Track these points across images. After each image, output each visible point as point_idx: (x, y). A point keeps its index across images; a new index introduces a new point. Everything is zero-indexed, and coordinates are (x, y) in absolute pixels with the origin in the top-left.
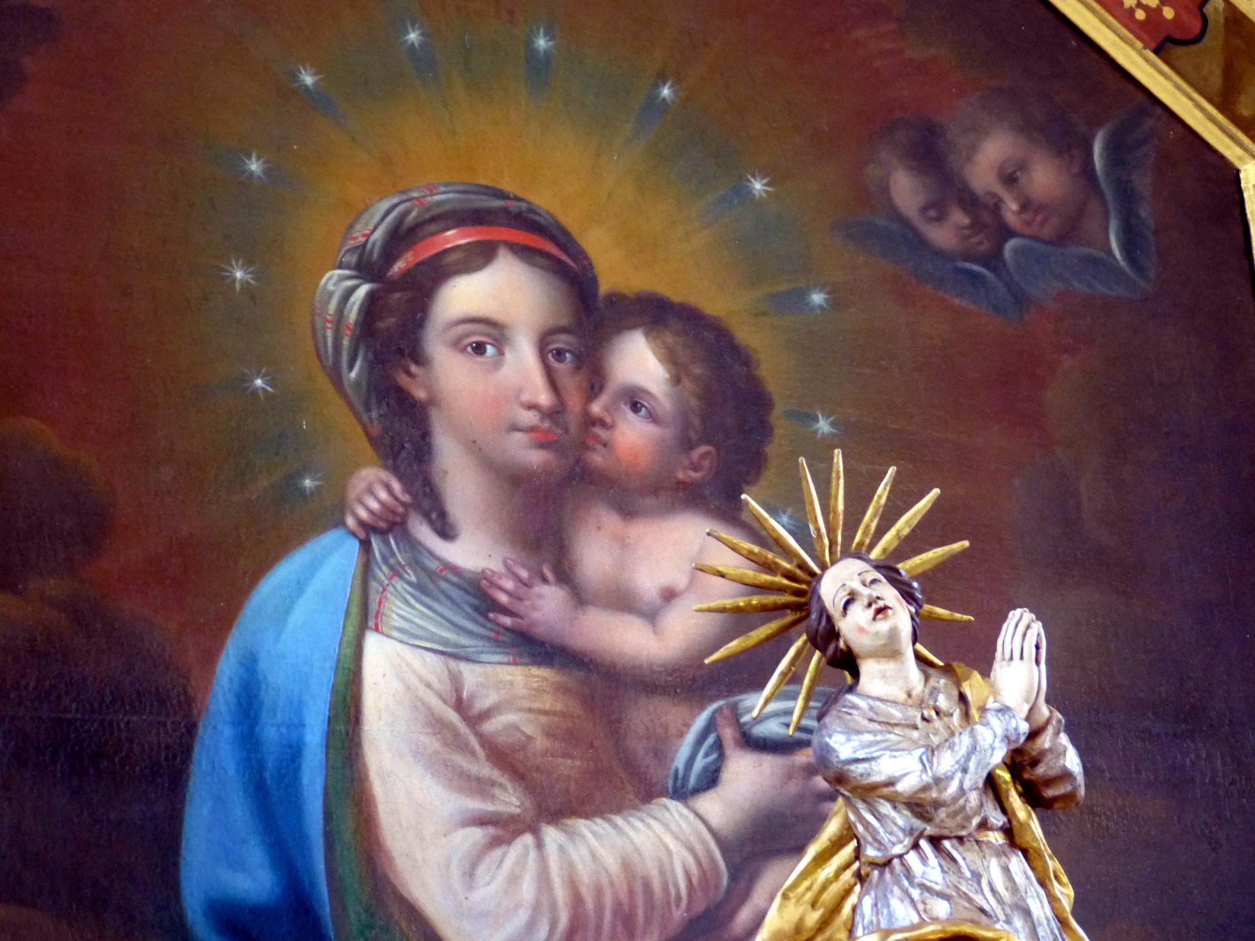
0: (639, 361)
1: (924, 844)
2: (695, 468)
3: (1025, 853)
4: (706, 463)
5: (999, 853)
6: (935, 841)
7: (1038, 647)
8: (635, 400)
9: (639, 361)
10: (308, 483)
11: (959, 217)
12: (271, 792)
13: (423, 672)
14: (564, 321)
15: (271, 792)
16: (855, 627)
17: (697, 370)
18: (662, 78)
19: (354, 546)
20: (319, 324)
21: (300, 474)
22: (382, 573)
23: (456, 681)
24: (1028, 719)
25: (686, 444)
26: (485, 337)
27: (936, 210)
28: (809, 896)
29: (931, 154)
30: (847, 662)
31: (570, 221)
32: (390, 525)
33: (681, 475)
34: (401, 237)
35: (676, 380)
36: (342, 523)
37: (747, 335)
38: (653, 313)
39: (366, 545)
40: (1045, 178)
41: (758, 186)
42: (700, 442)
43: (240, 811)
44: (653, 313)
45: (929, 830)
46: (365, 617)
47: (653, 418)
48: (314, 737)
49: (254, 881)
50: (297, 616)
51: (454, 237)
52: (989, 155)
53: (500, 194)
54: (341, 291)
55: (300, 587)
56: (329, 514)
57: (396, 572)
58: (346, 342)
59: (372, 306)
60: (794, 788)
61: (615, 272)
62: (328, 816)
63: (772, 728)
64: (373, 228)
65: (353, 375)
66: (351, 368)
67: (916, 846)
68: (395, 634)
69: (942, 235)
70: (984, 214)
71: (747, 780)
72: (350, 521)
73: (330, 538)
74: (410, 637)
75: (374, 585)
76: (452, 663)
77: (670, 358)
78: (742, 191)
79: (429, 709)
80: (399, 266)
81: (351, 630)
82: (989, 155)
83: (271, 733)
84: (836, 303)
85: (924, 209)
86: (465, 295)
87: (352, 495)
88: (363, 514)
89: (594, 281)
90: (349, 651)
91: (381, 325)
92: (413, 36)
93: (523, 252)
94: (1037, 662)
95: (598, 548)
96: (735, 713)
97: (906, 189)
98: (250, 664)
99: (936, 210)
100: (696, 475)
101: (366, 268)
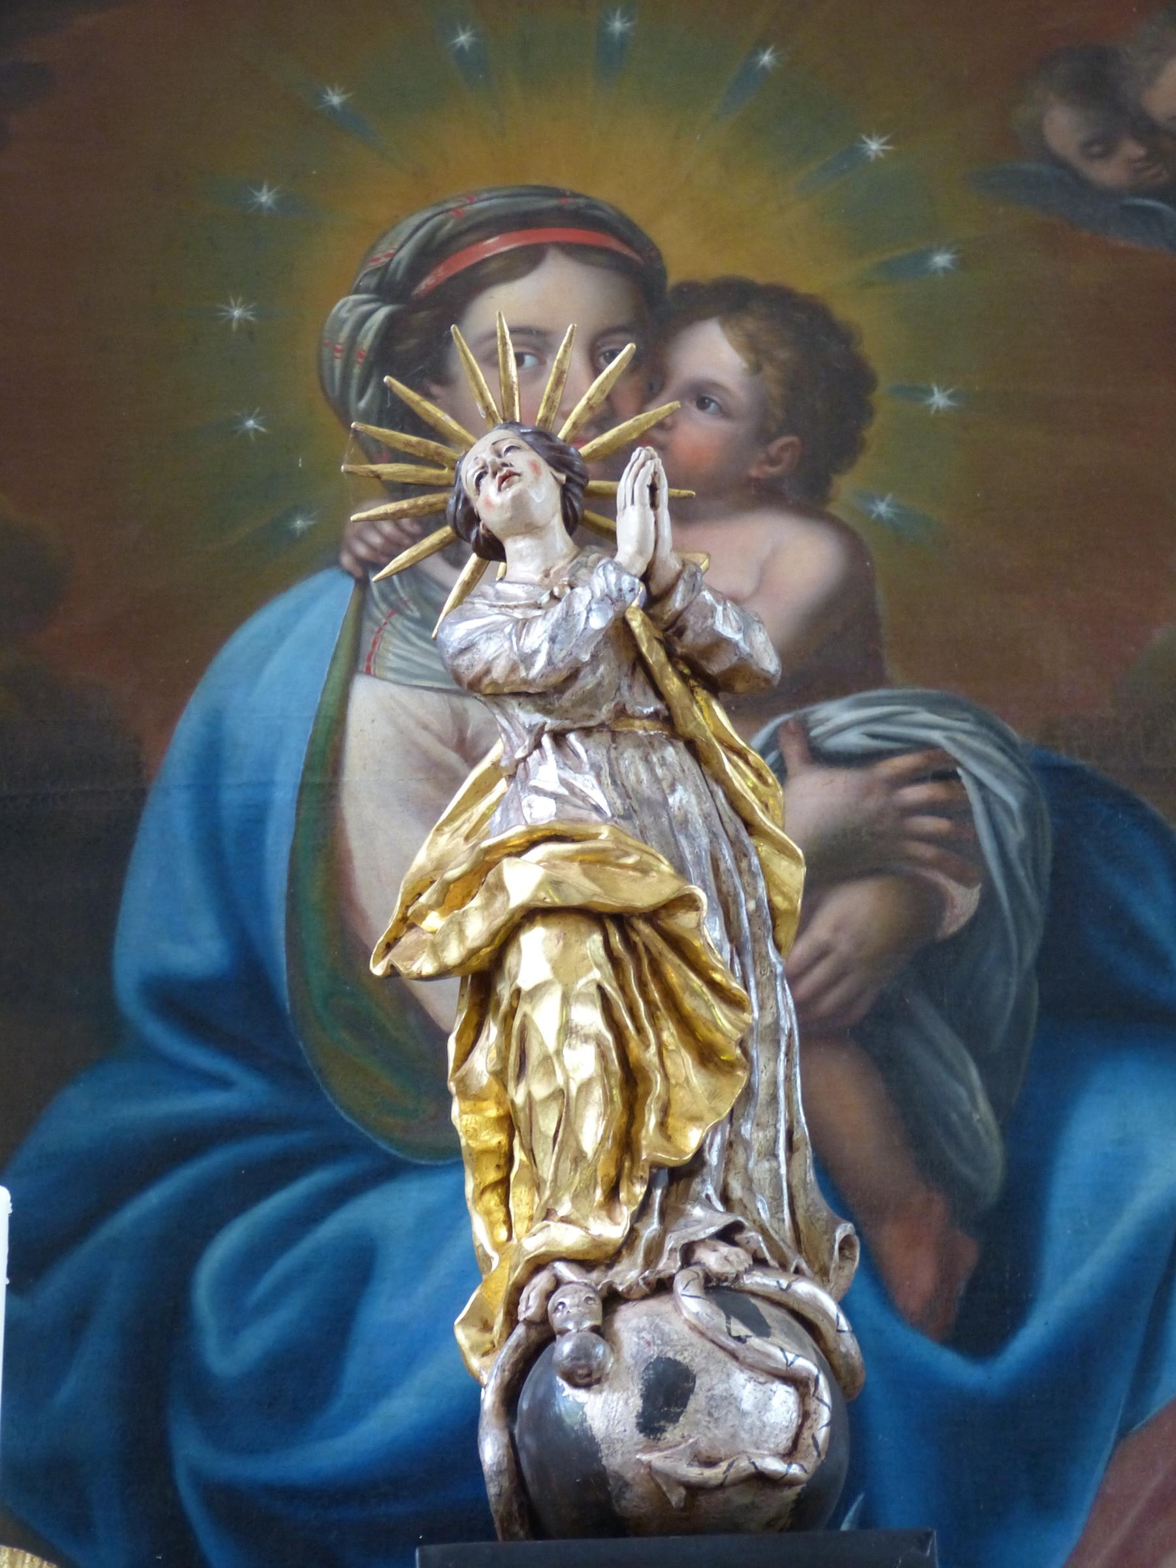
0: (713, 353)
1: (546, 741)
2: (772, 462)
3: (693, 747)
4: (787, 456)
5: (647, 746)
6: (559, 738)
7: (653, 489)
8: (702, 396)
9: (713, 353)
10: (299, 524)
11: (1132, 149)
12: (226, 854)
13: (421, 712)
14: (622, 320)
15: (226, 854)
16: (492, 503)
17: (783, 354)
18: (762, 45)
19: (349, 586)
20: (326, 352)
21: (290, 516)
22: (379, 611)
23: (460, 720)
24: (646, 578)
25: (763, 436)
27: (1102, 145)
28: (466, 829)
30: (492, 550)
31: (635, 211)
33: (754, 472)
34: (431, 252)
35: (756, 368)
36: (336, 563)
37: (848, 310)
38: (729, 299)
39: (363, 584)
41: (874, 146)
42: (780, 433)
43: (189, 877)
44: (729, 299)
45: (550, 723)
46: (355, 658)
47: (724, 413)
48: (284, 797)
49: (199, 951)
50: (275, 666)
51: (495, 245)
53: (557, 193)
54: (359, 317)
55: (281, 635)
56: (322, 552)
57: (396, 609)
58: (357, 370)
59: (390, 331)
60: (872, 804)
61: (686, 257)
62: (293, 878)
63: (853, 740)
64: (398, 249)
65: (362, 404)
66: (360, 396)
67: (538, 745)
68: (390, 675)
69: (1108, 173)
72: (346, 560)
73: (322, 579)
74: (407, 677)
75: (368, 625)
76: (457, 702)
77: (754, 349)
78: (854, 154)
79: (425, 754)
80: (427, 283)
81: (338, 674)
83: (232, 797)
84: (963, 262)
85: (1086, 146)
86: (503, 307)
87: (349, 532)
88: (362, 550)
89: (662, 273)
90: (332, 698)
91: (400, 348)
92: (463, 39)
93: (573, 251)
94: (654, 505)
96: (803, 728)
97: (1064, 127)
98: (215, 722)
99: (1102, 145)
100: (773, 470)
101: (386, 289)
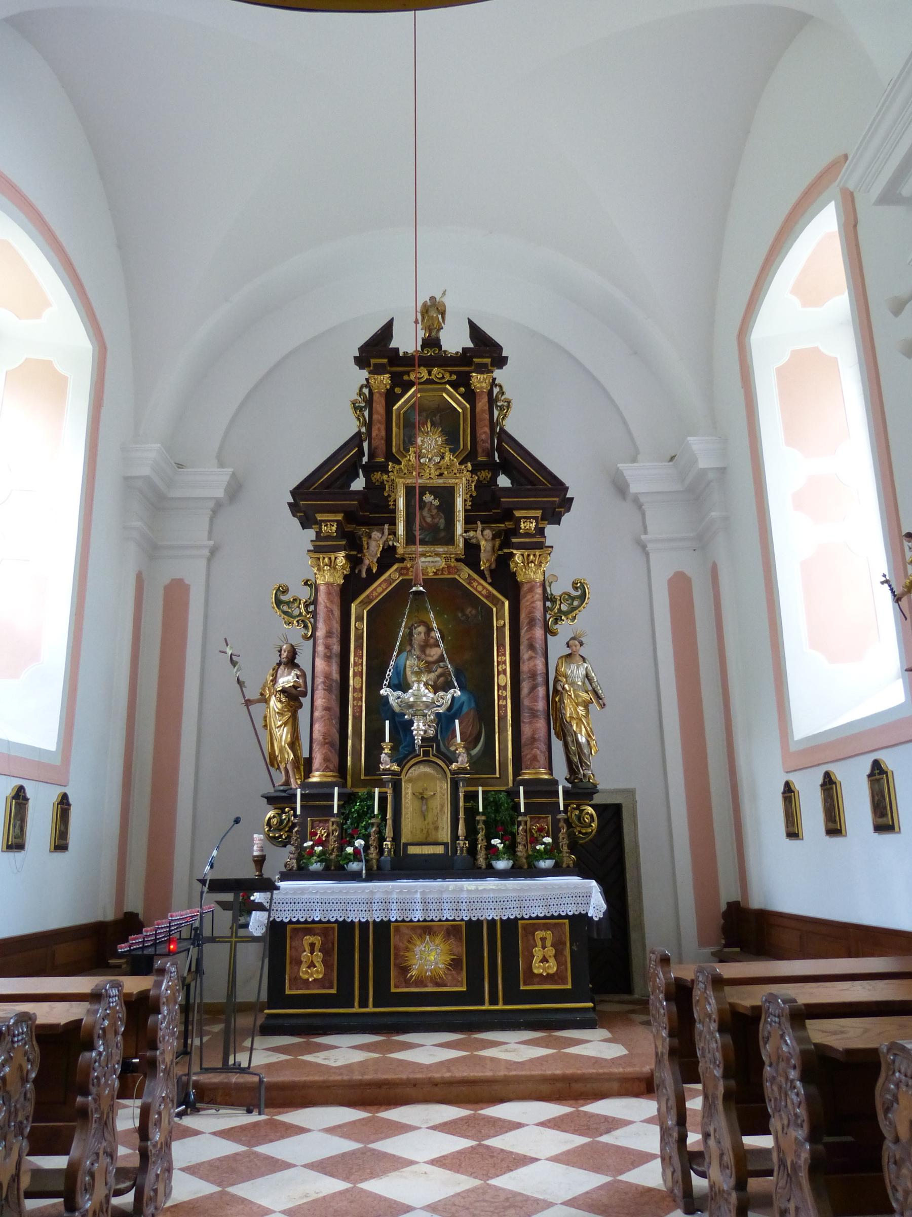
26: (420, 633)
29: (463, 611)
32: (410, 651)
40: (474, 612)
46: (407, 659)
52: (468, 610)
70: (468, 617)
71: (439, 670)
82: (468, 610)
95: (427, 652)
97: (460, 615)
